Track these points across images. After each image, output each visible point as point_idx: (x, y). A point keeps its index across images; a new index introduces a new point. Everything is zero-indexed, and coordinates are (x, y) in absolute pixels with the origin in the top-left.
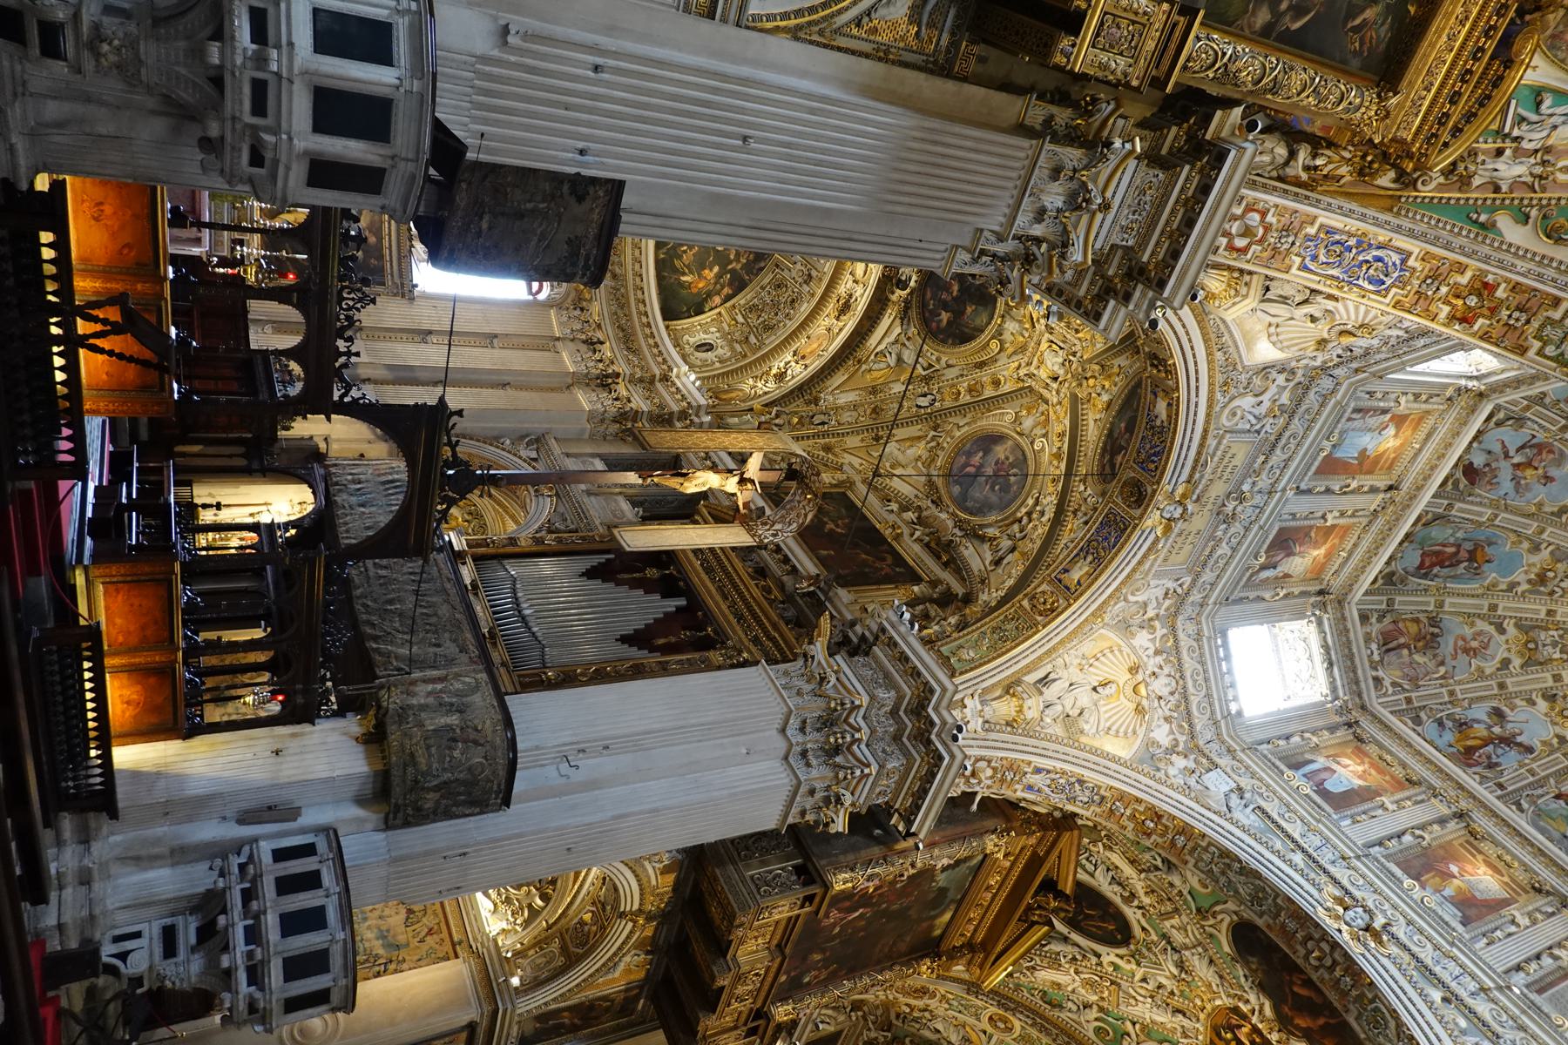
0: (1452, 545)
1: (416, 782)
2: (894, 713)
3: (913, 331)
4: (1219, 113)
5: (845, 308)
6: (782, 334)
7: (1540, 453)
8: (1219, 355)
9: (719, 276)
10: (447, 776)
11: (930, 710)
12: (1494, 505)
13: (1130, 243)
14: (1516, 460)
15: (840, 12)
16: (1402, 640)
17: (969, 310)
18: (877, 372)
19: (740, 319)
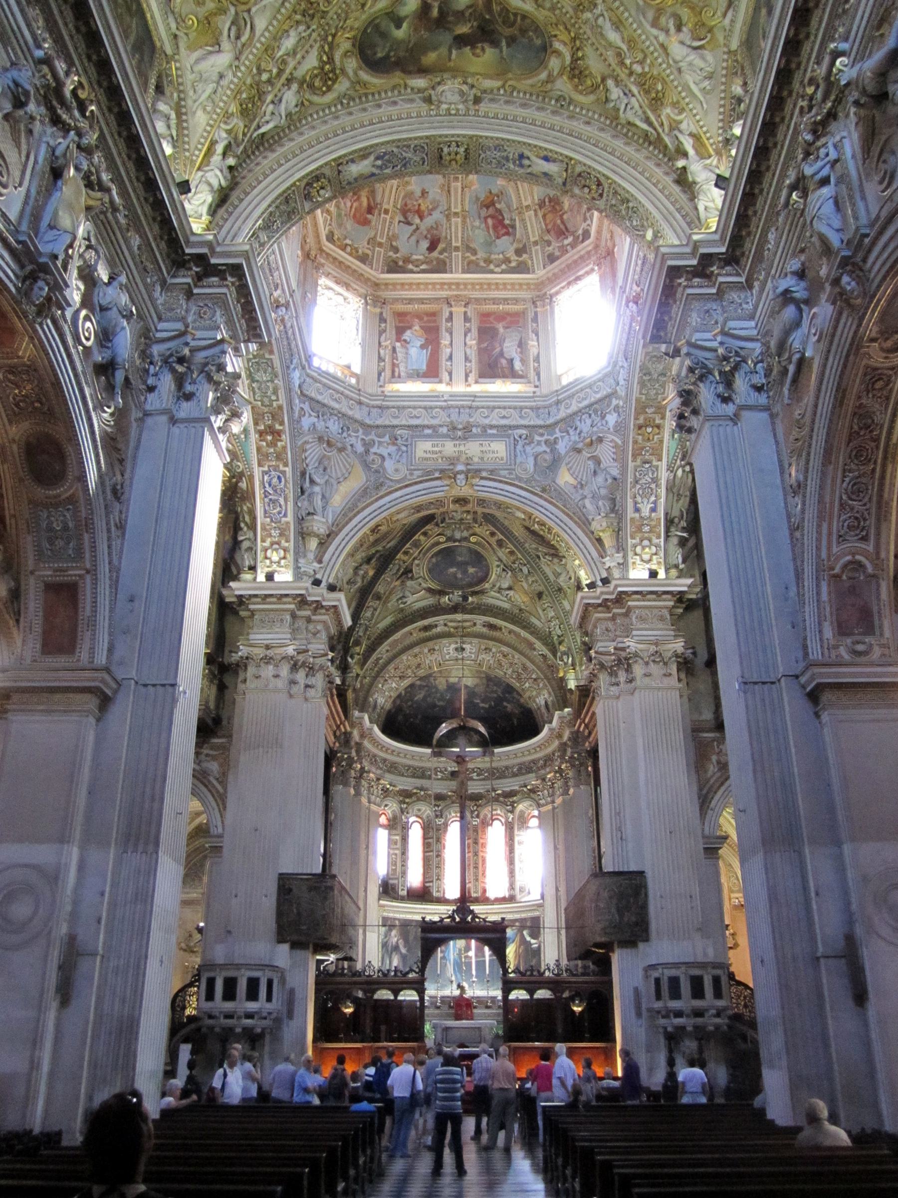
0: (486, 222)
1: (615, 927)
2: (613, 619)
3: (487, 586)
4: (227, 600)
5: (492, 627)
6: (525, 660)
7: (409, 210)
8: (361, 506)
9: (509, 702)
10: (613, 910)
11: (599, 601)
12: (448, 217)
13: (288, 617)
14: (417, 220)
15: (218, 792)
16: (559, 222)
17: (460, 559)
18: (520, 598)
19: (527, 685)
